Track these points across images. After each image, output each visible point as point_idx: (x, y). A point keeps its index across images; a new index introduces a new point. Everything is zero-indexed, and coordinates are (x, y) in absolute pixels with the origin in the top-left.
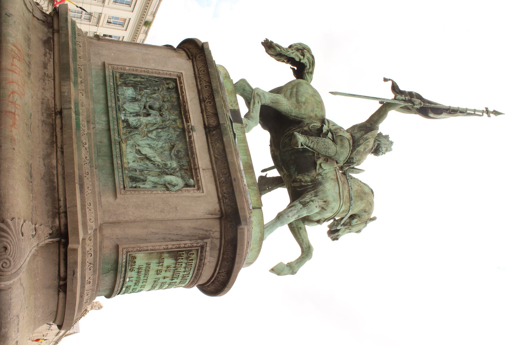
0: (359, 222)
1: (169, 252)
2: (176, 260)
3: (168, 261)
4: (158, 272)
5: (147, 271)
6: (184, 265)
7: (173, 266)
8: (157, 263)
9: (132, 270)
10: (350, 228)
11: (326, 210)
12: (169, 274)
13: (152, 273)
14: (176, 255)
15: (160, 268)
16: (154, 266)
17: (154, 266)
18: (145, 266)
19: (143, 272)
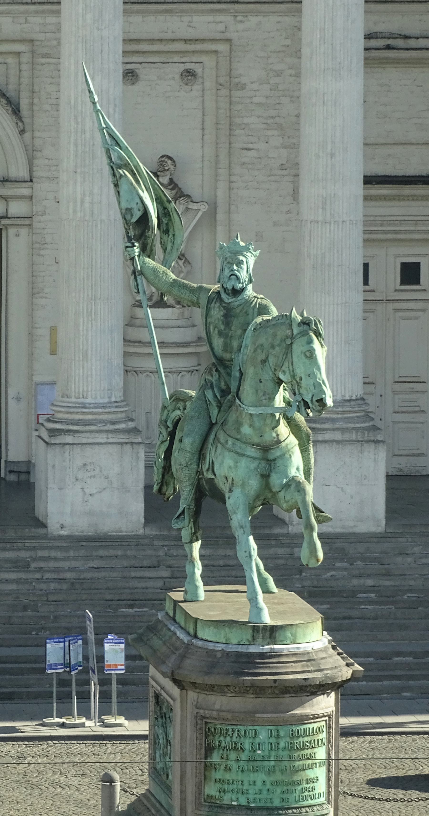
0: (283, 368)
1: (206, 758)
2: (214, 749)
3: (215, 757)
4: (228, 769)
5: (222, 781)
6: (222, 738)
7: (221, 751)
8: (216, 771)
9: (221, 799)
10: (298, 380)
11: (232, 478)
12: (233, 756)
13: (228, 776)
14: (209, 750)
15: (222, 767)
16: (219, 775)
17: (219, 775)
18: (218, 785)
19: (226, 787)
